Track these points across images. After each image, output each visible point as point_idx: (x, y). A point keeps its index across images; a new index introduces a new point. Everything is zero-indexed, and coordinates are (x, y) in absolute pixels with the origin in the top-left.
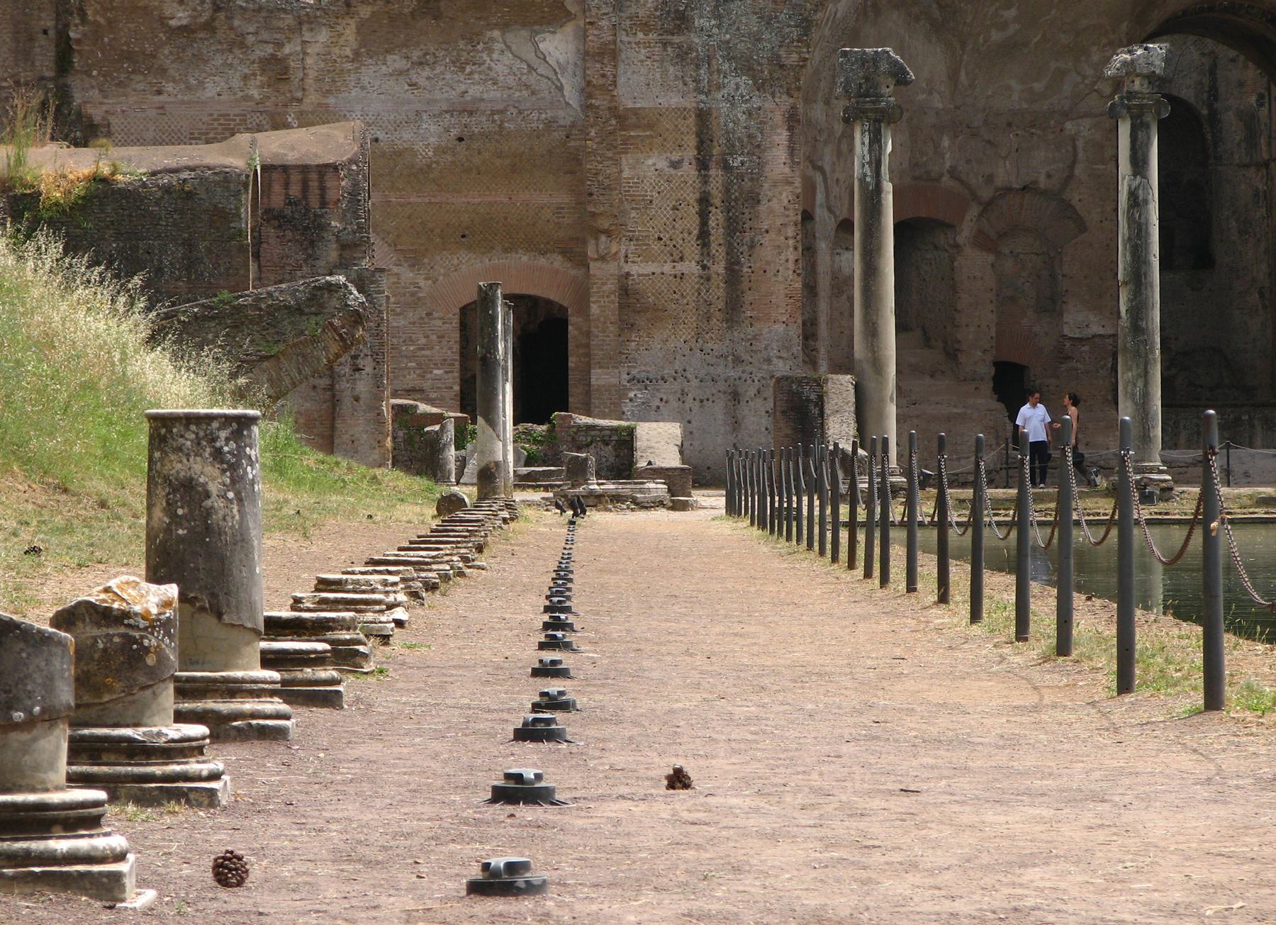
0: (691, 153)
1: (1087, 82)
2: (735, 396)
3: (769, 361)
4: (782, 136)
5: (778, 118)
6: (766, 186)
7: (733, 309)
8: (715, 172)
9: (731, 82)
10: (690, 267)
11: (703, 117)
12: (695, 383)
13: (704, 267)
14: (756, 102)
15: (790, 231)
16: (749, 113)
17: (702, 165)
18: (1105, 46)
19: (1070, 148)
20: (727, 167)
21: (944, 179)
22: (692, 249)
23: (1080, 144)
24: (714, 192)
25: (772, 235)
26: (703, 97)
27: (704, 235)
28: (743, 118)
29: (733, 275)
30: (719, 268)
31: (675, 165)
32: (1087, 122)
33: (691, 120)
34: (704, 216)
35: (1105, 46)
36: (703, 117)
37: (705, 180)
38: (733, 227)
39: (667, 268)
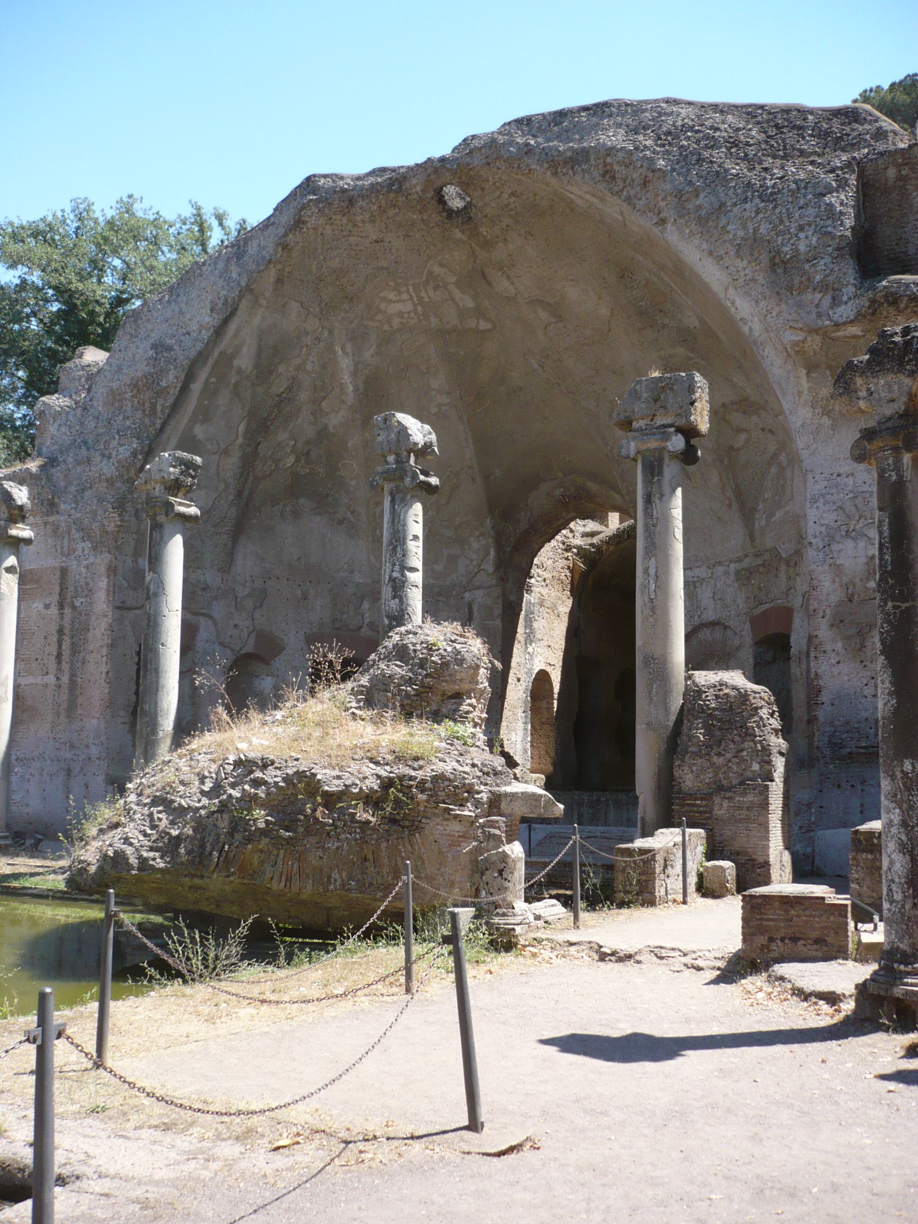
0: (55, 598)
1: (474, 563)
2: (69, 772)
3: (87, 746)
4: (103, 583)
5: (102, 569)
6: (93, 618)
7: (72, 706)
8: (67, 610)
9: (81, 545)
10: (51, 679)
11: (64, 571)
12: (49, 762)
13: (58, 679)
14: (92, 559)
15: (104, 651)
16: (87, 567)
17: (61, 606)
18: (478, 537)
19: (467, 610)
20: (74, 607)
21: (363, 630)
22: (52, 665)
23: (475, 608)
24: (66, 625)
25: (94, 655)
26: (64, 559)
27: (59, 656)
28: (84, 570)
29: (73, 685)
30: (65, 679)
31: (47, 606)
32: (480, 593)
33: (58, 573)
34: (60, 643)
35: (478, 537)
36: (64, 571)
37: (62, 616)
38: (75, 650)
39: (39, 680)
